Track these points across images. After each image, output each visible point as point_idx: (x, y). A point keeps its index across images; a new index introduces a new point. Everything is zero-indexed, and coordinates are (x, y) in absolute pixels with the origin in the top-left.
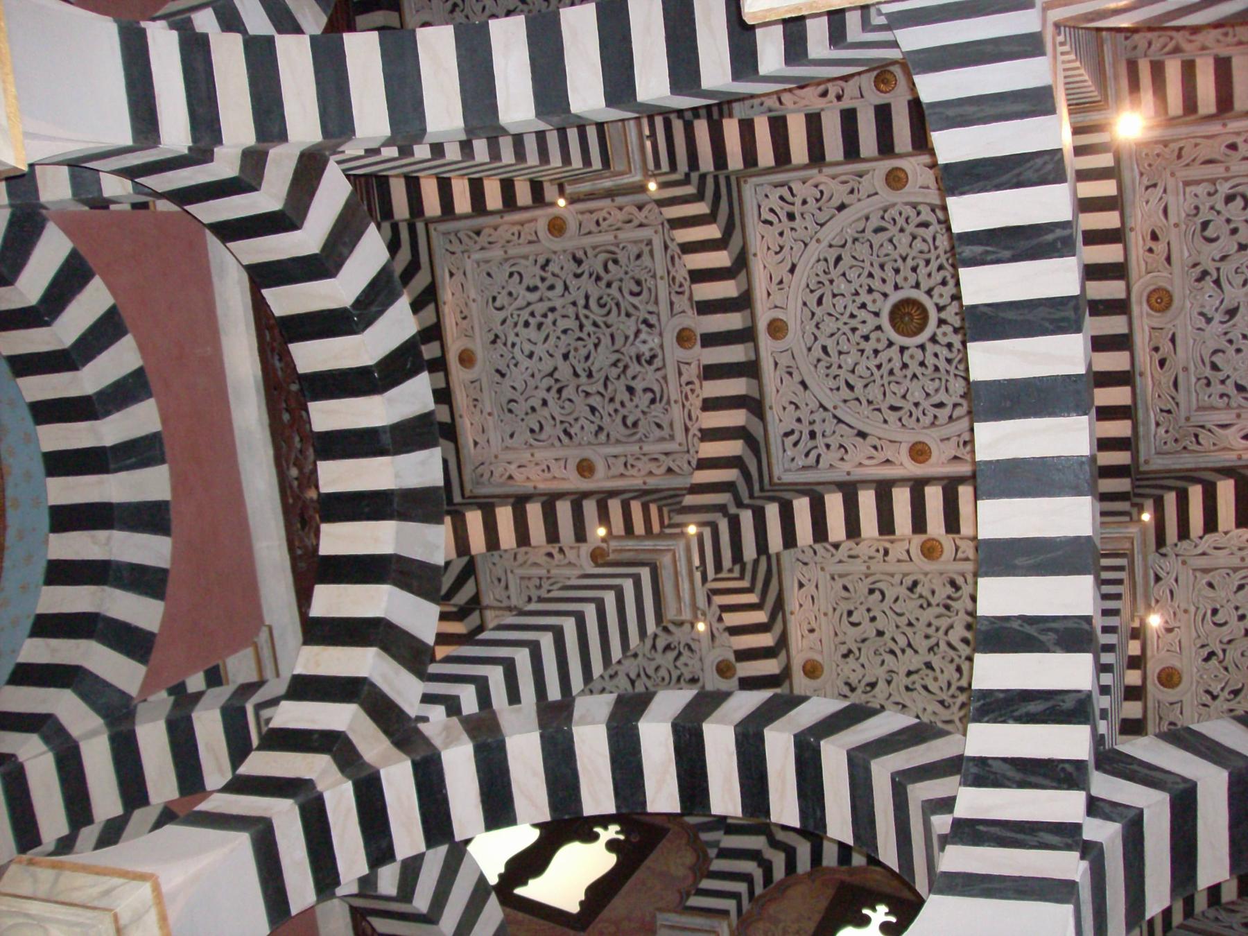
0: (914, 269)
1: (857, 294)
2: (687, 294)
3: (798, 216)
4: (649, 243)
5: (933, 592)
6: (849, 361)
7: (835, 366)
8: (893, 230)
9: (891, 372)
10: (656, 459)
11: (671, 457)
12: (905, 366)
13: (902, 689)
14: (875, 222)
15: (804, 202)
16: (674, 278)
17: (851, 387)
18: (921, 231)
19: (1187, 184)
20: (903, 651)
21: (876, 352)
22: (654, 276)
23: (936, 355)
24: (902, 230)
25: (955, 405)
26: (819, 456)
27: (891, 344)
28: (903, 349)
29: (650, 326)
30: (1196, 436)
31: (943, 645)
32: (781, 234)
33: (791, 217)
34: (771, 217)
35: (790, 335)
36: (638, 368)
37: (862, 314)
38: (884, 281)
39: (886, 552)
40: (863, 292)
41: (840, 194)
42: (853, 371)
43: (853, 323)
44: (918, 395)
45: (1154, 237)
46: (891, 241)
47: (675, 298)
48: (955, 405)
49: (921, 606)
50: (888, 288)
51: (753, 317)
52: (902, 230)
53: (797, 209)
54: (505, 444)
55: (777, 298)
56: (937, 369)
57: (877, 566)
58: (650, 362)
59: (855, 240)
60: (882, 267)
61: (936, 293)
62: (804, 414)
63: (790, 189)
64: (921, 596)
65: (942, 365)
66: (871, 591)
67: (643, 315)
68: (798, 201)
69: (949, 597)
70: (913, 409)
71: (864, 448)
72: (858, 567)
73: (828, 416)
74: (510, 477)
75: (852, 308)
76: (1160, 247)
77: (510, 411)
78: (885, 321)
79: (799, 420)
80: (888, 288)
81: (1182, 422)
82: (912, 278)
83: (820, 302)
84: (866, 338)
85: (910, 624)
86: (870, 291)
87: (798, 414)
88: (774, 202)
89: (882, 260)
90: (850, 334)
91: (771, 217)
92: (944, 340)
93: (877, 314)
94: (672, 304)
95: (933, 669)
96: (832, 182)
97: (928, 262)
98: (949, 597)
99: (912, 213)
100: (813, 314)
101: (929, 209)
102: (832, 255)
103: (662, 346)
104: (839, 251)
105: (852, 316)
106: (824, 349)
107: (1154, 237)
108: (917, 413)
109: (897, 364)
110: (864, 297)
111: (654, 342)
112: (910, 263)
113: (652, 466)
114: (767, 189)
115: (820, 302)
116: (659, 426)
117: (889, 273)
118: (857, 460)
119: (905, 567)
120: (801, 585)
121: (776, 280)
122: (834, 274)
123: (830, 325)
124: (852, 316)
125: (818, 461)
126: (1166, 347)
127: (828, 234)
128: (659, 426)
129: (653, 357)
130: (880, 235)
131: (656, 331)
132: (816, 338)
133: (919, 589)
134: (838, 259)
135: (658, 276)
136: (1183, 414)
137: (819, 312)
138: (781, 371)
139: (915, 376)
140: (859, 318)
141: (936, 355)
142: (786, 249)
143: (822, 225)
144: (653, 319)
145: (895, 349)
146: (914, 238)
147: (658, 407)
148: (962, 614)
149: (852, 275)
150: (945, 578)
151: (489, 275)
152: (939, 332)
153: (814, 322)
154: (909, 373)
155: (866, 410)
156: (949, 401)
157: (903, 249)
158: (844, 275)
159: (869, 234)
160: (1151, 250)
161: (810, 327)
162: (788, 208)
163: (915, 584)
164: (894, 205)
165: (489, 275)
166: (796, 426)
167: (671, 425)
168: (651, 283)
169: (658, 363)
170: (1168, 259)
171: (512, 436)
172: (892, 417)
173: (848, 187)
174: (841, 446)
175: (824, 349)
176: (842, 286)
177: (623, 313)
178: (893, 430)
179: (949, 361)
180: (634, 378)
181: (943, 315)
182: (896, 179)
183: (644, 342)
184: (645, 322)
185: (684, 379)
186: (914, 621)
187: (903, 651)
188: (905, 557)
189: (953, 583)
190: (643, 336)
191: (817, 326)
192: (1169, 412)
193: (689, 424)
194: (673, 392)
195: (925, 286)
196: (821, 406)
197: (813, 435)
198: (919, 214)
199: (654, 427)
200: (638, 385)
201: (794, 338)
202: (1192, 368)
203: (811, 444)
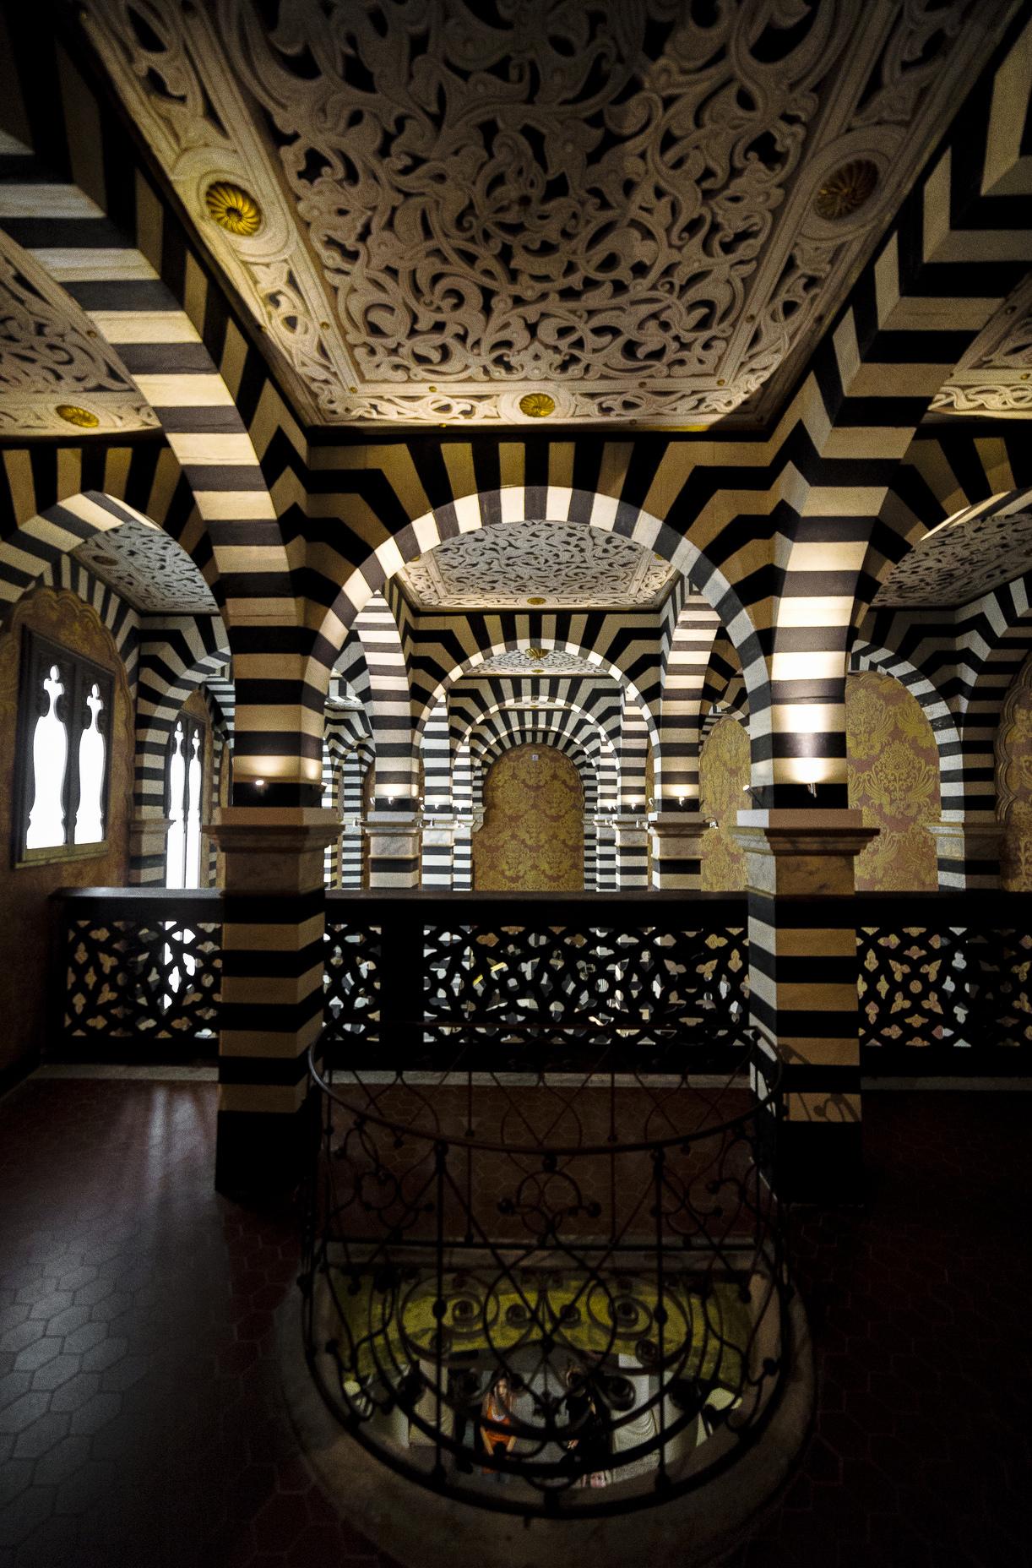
13: (481, 115)
20: (596, 120)
31: (607, 215)
49: (708, 173)
64: (734, 173)
85: (668, 141)
95: (546, 198)
186: (672, 155)
187: (596, 120)
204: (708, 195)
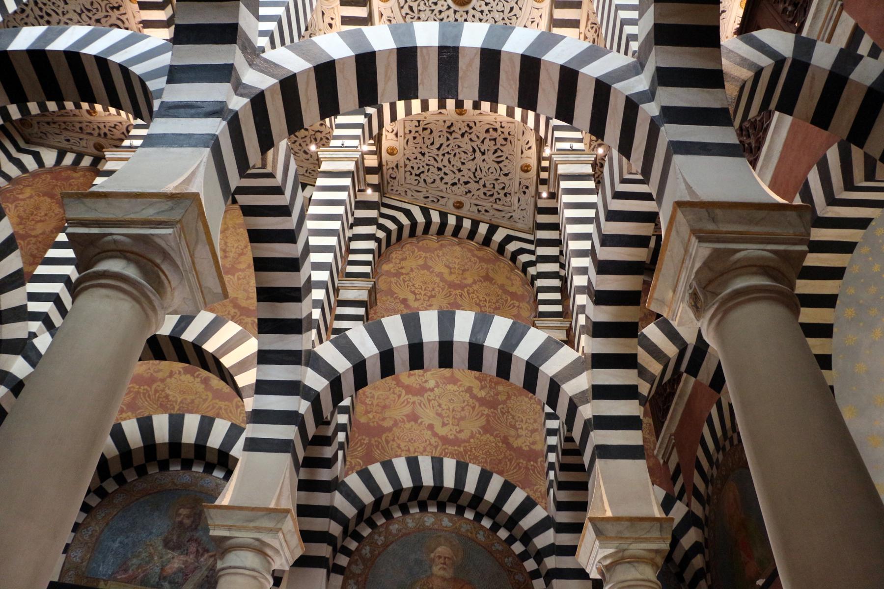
1: (489, 11)
2: (590, 22)
16: (596, 31)
38: (474, 16)
45: (331, 25)
61: (446, 7)
76: (328, 20)
82: (458, 16)
83: (512, 9)
86: (482, 12)
110: (484, 8)
115: (512, 9)
121: (535, 24)
160: (332, 19)
195: (451, 11)
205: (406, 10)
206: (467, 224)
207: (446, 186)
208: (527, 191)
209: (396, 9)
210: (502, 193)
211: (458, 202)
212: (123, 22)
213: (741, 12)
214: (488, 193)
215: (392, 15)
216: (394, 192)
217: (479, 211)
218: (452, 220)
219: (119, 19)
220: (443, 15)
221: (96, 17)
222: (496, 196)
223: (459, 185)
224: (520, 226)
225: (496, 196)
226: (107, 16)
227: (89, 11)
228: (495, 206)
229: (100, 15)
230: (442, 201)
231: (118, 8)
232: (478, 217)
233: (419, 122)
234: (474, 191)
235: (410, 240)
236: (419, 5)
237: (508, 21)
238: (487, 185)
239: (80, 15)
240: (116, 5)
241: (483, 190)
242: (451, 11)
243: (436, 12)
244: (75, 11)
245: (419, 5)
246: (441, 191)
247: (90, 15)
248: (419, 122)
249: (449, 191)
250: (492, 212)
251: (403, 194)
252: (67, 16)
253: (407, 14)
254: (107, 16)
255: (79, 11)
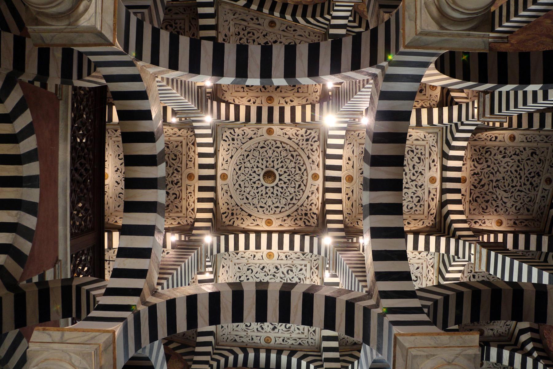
0: (273, 162)
1: (253, 168)
3: (235, 140)
4: (181, 142)
5: (270, 271)
6: (248, 190)
7: (243, 191)
8: (267, 148)
9: (262, 195)
10: (174, 219)
11: (180, 219)
12: (267, 193)
14: (262, 144)
15: (238, 135)
16: (189, 156)
17: (247, 199)
18: (277, 149)
19: (360, 144)
21: (257, 188)
22: (182, 154)
23: (277, 190)
24: (270, 148)
25: (282, 208)
26: (234, 222)
27: (262, 186)
28: (266, 188)
29: (178, 171)
30: (357, 222)
32: (229, 145)
33: (233, 140)
34: (226, 139)
35: (228, 180)
36: (171, 186)
37: (254, 175)
38: (262, 164)
39: (254, 256)
40: (255, 167)
41: (251, 134)
42: (249, 194)
43: (251, 177)
44: (270, 203)
45: (349, 159)
46: (266, 151)
47: (188, 162)
48: (282, 208)
50: (264, 167)
51: (216, 172)
52: (270, 148)
53: (235, 137)
54: (116, 209)
55: (225, 166)
56: (277, 195)
57: (251, 261)
58: (176, 184)
59: (254, 150)
60: (262, 160)
62: (230, 207)
63: (234, 130)
64: (265, 272)
65: (279, 194)
66: (248, 270)
67: (176, 167)
68: (236, 135)
69: (275, 272)
70: (268, 208)
71: (250, 220)
72: (244, 261)
73: (239, 208)
74: (116, 222)
75: (251, 172)
76: (351, 163)
77: (119, 197)
78: (261, 177)
79: (228, 209)
80: (264, 167)
81: (353, 218)
83: (240, 169)
84: (255, 183)
87: (228, 206)
88: (228, 134)
89: (263, 157)
90: (249, 181)
91: (226, 139)
92: (280, 186)
93: (259, 175)
94: (187, 164)
96: (248, 130)
97: (278, 160)
98: (275, 272)
99: (274, 143)
100: (237, 173)
101: (279, 143)
102: (246, 154)
103: (181, 179)
104: (249, 153)
105: (250, 175)
106: (240, 185)
107: (349, 159)
108: (269, 209)
109: (264, 192)
110: (256, 170)
111: (179, 177)
112: (272, 159)
113: (173, 221)
114: (226, 129)
115: (240, 169)
116: (177, 207)
117: (264, 162)
118: (248, 224)
119: (261, 262)
120: (223, 267)
121: (225, 160)
122: (246, 160)
123: (242, 177)
124: (250, 175)
125: (233, 223)
126: (350, 194)
127: (245, 147)
128: (177, 207)
129: (178, 182)
130: (263, 149)
131: (180, 173)
132: (237, 181)
133: (265, 269)
134: (248, 155)
135: (183, 153)
136: (354, 215)
137: (239, 172)
138: (224, 191)
139: (270, 197)
140: (253, 176)
141: (277, 190)
142: (230, 151)
143: (243, 144)
144: (179, 169)
145: (264, 187)
146: (274, 151)
147: (177, 200)
148: (279, 278)
149: (252, 161)
150: (274, 266)
151: (118, 146)
152: (279, 183)
153: (237, 176)
154: (268, 196)
155: (252, 207)
156: (280, 206)
157: (270, 155)
158: (249, 161)
159: (259, 148)
160: (348, 163)
161: (236, 177)
162: (233, 137)
163: (264, 267)
164: (268, 140)
165: (118, 146)
166: (227, 211)
167: (181, 207)
168: (180, 156)
169: (179, 184)
170: (353, 167)
171: (119, 206)
172: (261, 210)
173: (254, 132)
174: (242, 219)
175: (240, 185)
176: (248, 165)
177: (168, 165)
178: (260, 214)
179: (281, 193)
180: (170, 189)
181: (281, 178)
182: (270, 132)
183: (175, 177)
184: (176, 170)
185: (188, 191)
188: (261, 258)
189: (276, 268)
190: (175, 175)
191: (238, 177)
192: (350, 214)
193: (188, 207)
194: (184, 195)
195: (276, 167)
196: (237, 204)
197: (232, 214)
198: (276, 144)
199: (175, 207)
200: (171, 192)
201: (229, 181)
202: (357, 201)
203: (231, 217)
204: (268, 275)
205: (303, 169)
206: (266, 11)
207: (281, 40)
208: (224, 38)
209: (309, 169)
210: (241, 35)
211: (271, 26)
212: (474, 165)
213: (106, 171)
214: (251, 35)
215: (311, 165)
216: (318, 35)
217: (257, 19)
218: (277, 14)
219: (476, 167)
220: (280, 165)
221: (489, 169)
222: (246, 32)
223: (272, 41)
224: (228, 7)
225: (246, 32)
226: (483, 169)
227: (492, 173)
228: (246, 24)
229: (486, 171)
230: (284, 27)
231: (475, 174)
232: (258, 14)
233: (298, 92)
234: (261, 36)
235: (307, 4)
236: (295, 171)
237: (242, 161)
238: (252, 42)
239: (498, 171)
240: (475, 176)
241: (255, 37)
242: (276, 168)
243: (285, 167)
244: (500, 173)
245: (295, 171)
246: (284, 36)
247: (492, 170)
248: (298, 92)
249: (279, 36)
250: (248, 18)
251: (312, 33)
252: (506, 170)
253: (302, 166)
254: (483, 169)
255: (498, 173)
